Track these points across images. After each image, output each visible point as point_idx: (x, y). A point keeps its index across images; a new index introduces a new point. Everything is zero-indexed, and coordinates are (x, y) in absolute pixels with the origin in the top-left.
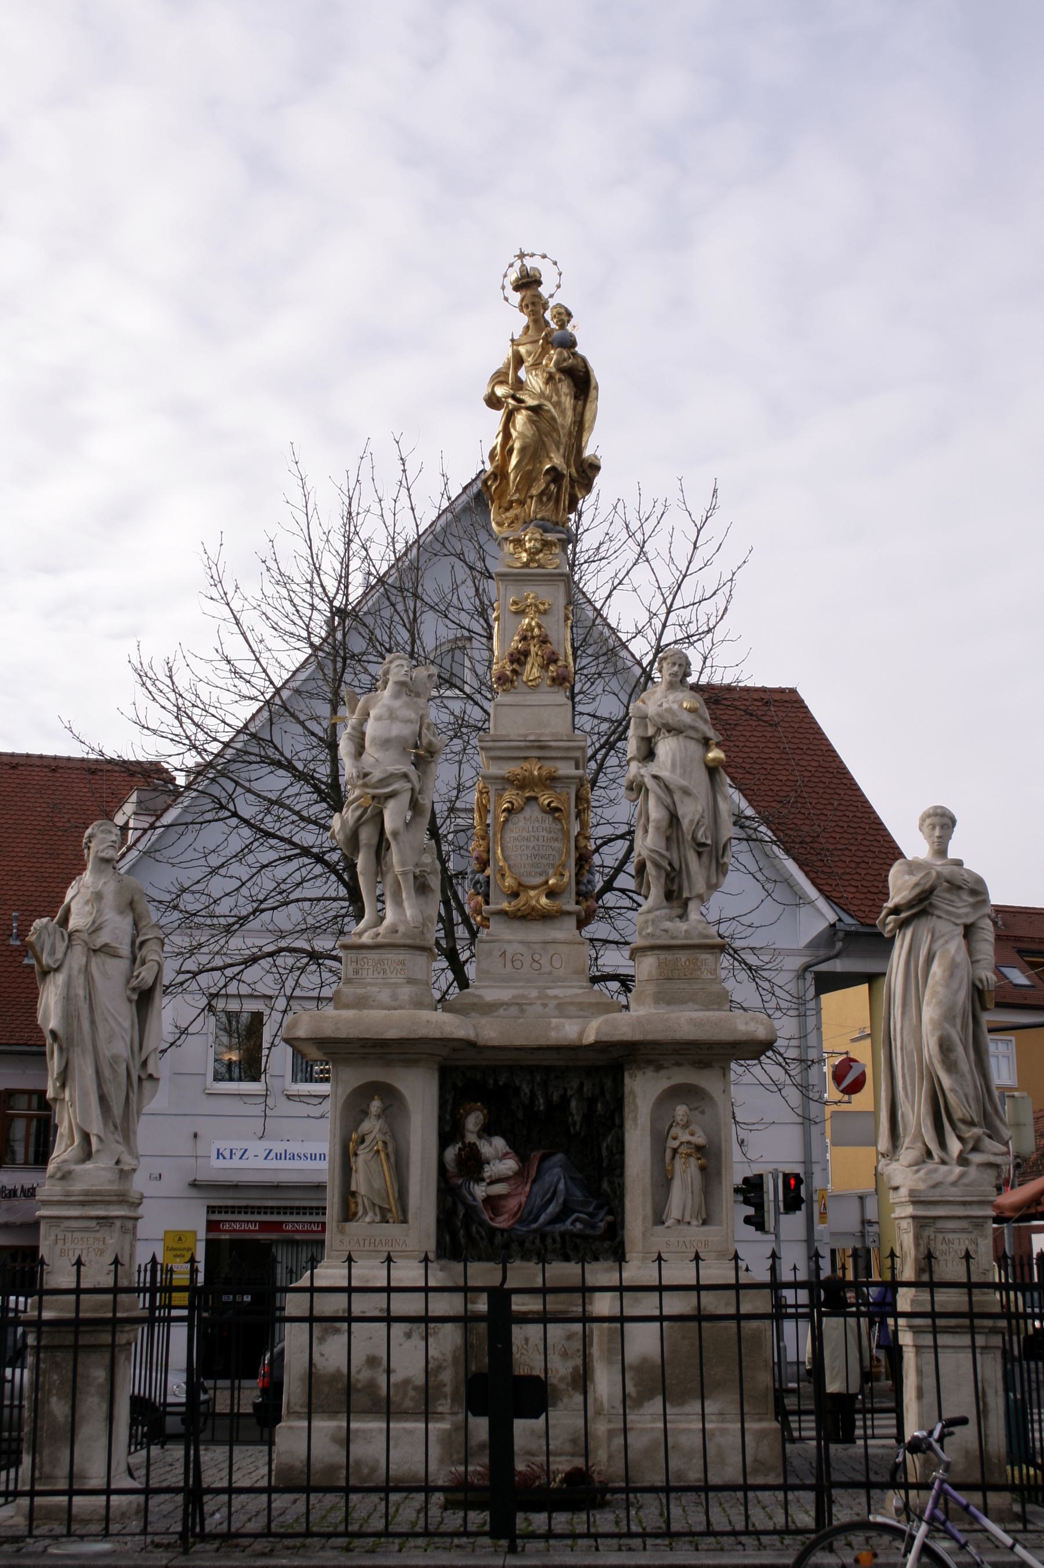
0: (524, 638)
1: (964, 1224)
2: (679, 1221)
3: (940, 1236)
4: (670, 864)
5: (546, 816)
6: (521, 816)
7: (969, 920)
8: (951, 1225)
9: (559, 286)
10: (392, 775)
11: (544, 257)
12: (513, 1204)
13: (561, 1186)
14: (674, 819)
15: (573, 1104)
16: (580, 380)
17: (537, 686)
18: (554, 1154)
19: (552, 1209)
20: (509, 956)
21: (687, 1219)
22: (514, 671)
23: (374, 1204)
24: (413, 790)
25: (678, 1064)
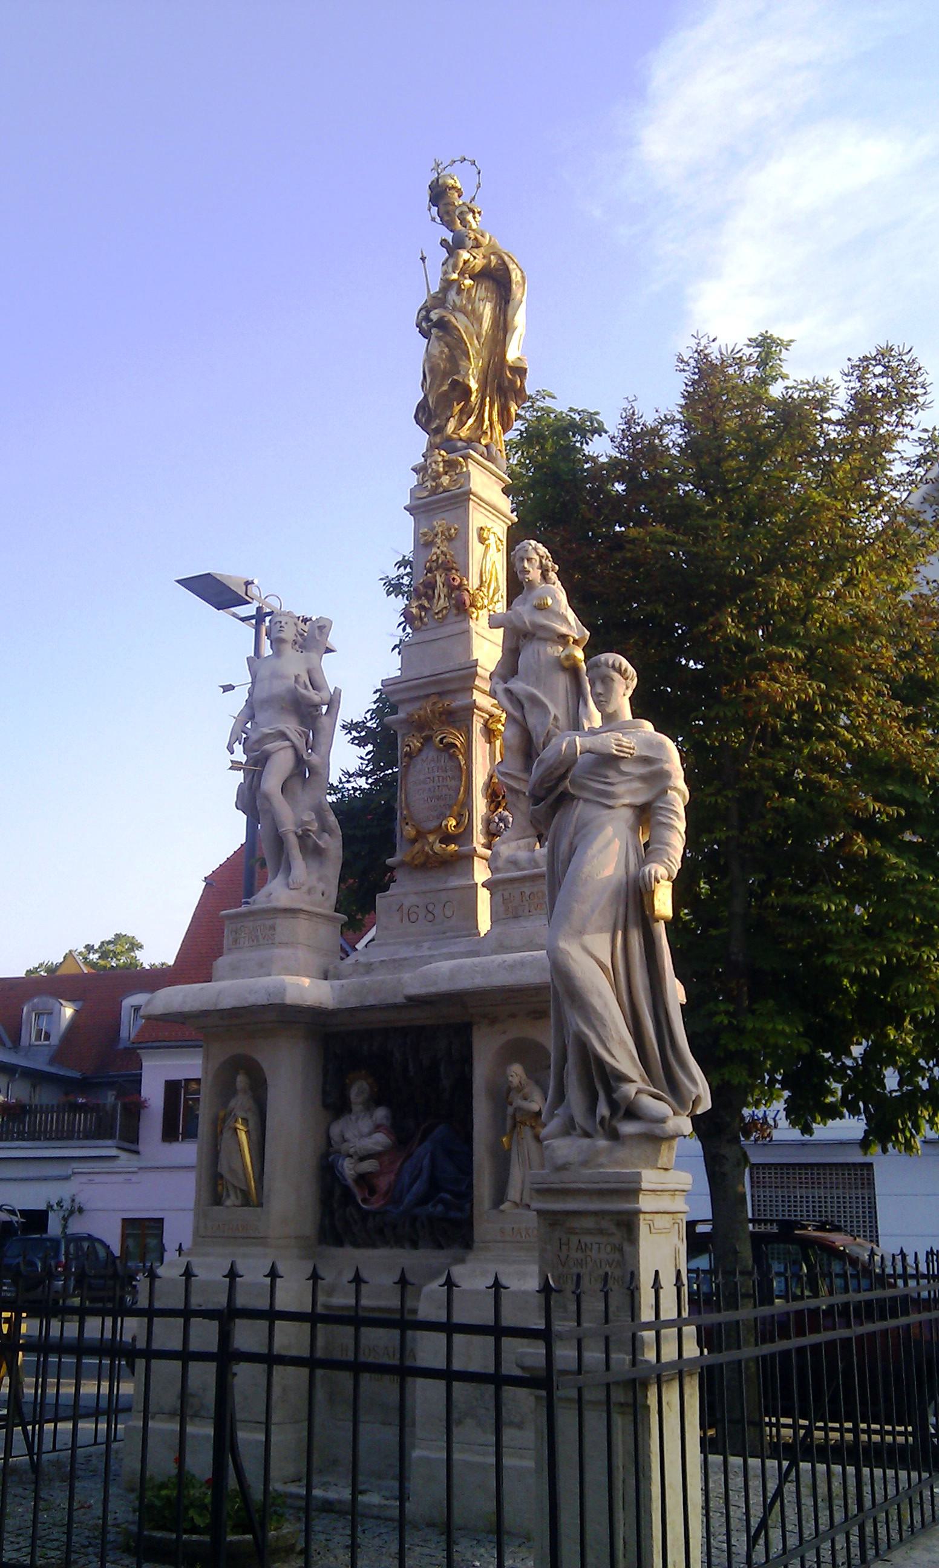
3: (574, 1239)
5: (443, 754)
6: (419, 759)
7: (639, 800)
9: (479, 187)
10: (267, 736)
13: (426, 1162)
15: (442, 1069)
17: (444, 617)
20: (405, 911)
22: (421, 607)
23: (235, 1187)
24: (294, 747)
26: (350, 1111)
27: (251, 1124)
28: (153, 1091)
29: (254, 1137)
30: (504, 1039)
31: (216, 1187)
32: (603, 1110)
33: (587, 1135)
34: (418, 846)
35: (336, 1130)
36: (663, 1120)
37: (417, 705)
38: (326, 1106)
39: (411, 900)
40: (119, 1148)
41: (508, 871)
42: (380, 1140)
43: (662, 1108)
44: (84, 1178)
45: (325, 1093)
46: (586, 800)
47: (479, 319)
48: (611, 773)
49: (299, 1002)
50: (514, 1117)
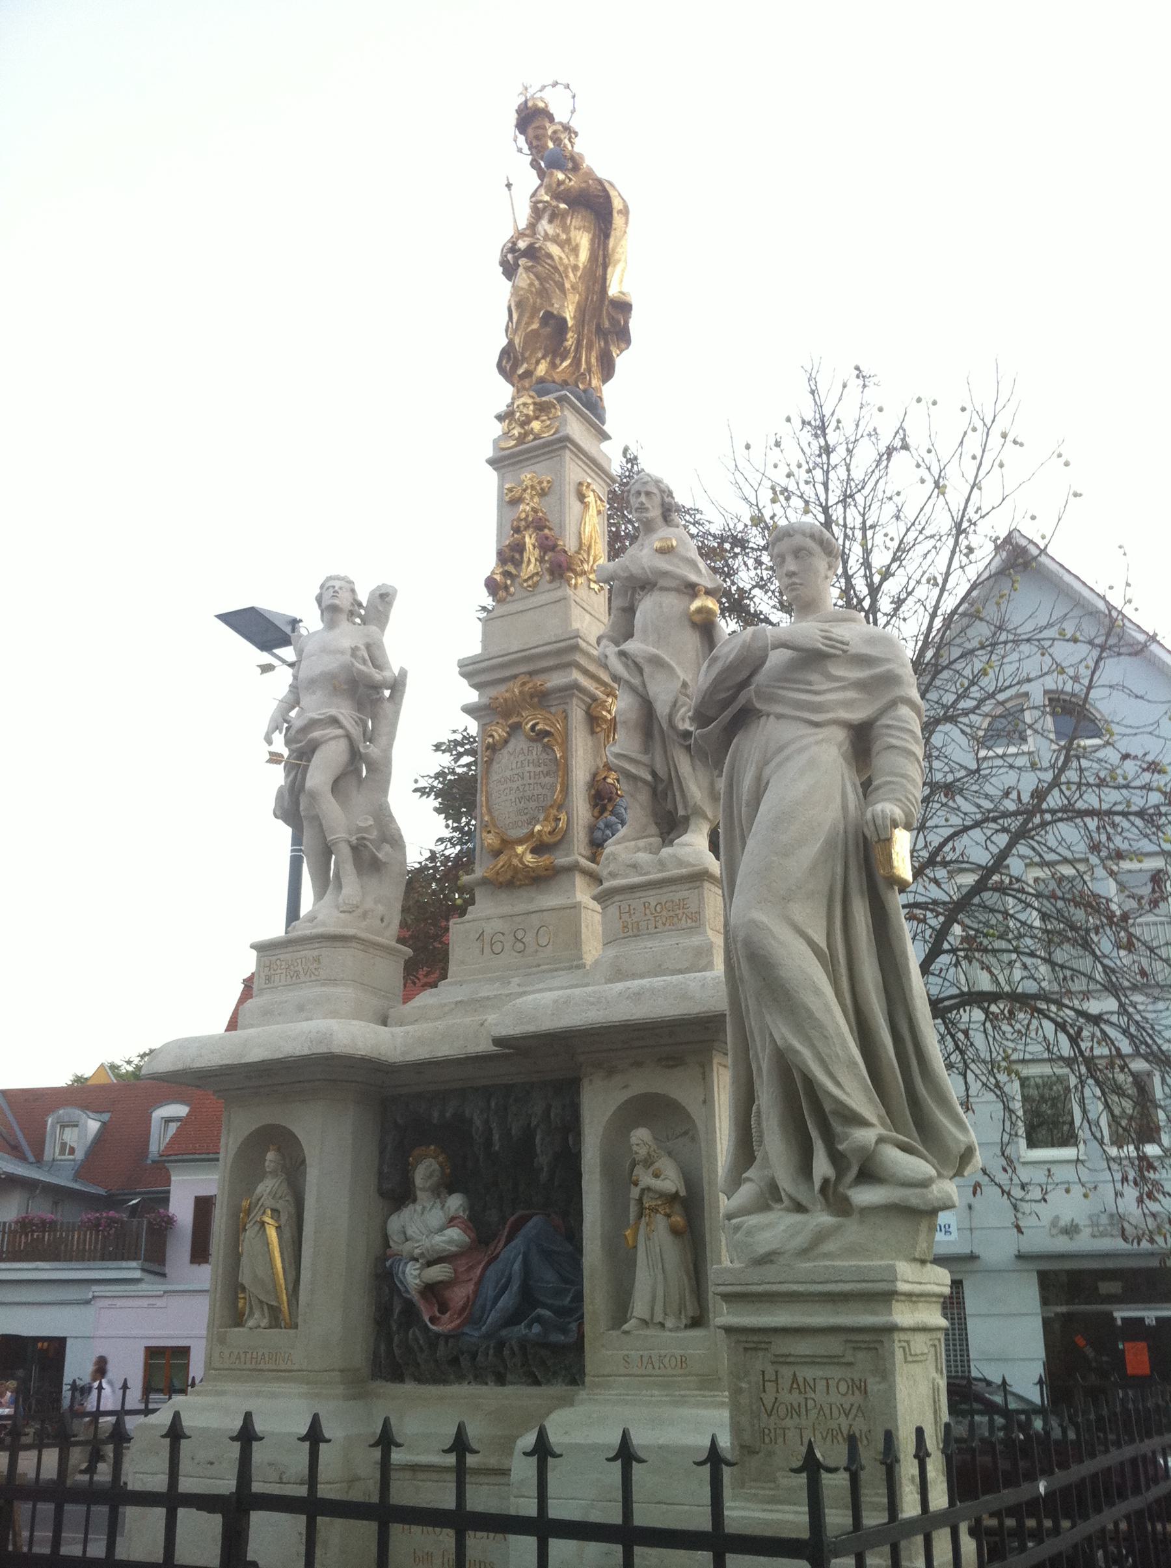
0: (517, 530)
1: (833, 1345)
2: (645, 1323)
3: (786, 1372)
4: (654, 774)
5: (534, 745)
6: (504, 751)
7: (857, 715)
8: (803, 1347)
9: (573, 112)
11: (555, 84)
12: (459, 1295)
13: (517, 1266)
14: (647, 707)
15: (538, 1138)
16: (594, 206)
17: (535, 585)
18: (530, 1217)
19: (506, 1301)
20: (487, 938)
21: (659, 1318)
22: (507, 574)
23: (261, 1302)
25: (638, 1064)
28: (181, 1208)
29: (287, 1235)
30: (622, 1096)
31: (234, 1305)
32: (822, 1167)
33: (800, 1208)
34: (503, 858)
35: (395, 1223)
37: (502, 688)
38: (382, 1194)
39: (490, 928)
40: (143, 1270)
43: (917, 1166)
44: (107, 1302)
46: (779, 717)
47: (575, 250)
48: (814, 677)
49: (349, 1051)
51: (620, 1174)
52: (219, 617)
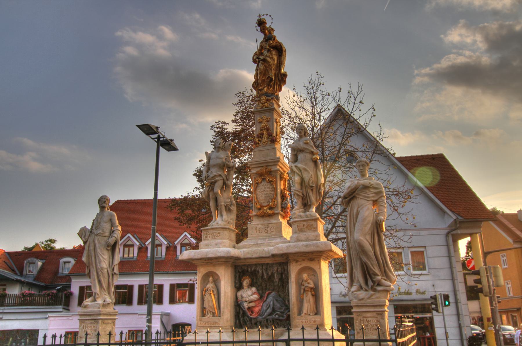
0: (262, 130)
1: (374, 314)
2: (306, 314)
3: (365, 319)
4: (303, 194)
7: (374, 199)
8: (369, 314)
10: (215, 176)
11: (267, 15)
12: (257, 309)
13: (271, 303)
14: (302, 180)
15: (275, 275)
16: (280, 50)
18: (272, 292)
19: (269, 311)
21: (309, 313)
22: (259, 140)
24: (223, 179)
25: (303, 260)
26: (243, 288)
27: (215, 292)
28: (75, 289)
29: (216, 296)
30: (301, 267)
31: (203, 312)
32: (370, 283)
33: (366, 290)
34: (261, 211)
35: (239, 294)
36: (390, 286)
37: (259, 169)
38: (235, 287)
39: (258, 227)
40: (63, 308)
41: (298, 218)
42: (256, 296)
43: (388, 283)
44: (52, 318)
45: (235, 283)
46: (361, 198)
47: (274, 60)
48: (367, 191)
49: (234, 255)
50: (304, 289)
51: (300, 284)
52: (139, 126)
